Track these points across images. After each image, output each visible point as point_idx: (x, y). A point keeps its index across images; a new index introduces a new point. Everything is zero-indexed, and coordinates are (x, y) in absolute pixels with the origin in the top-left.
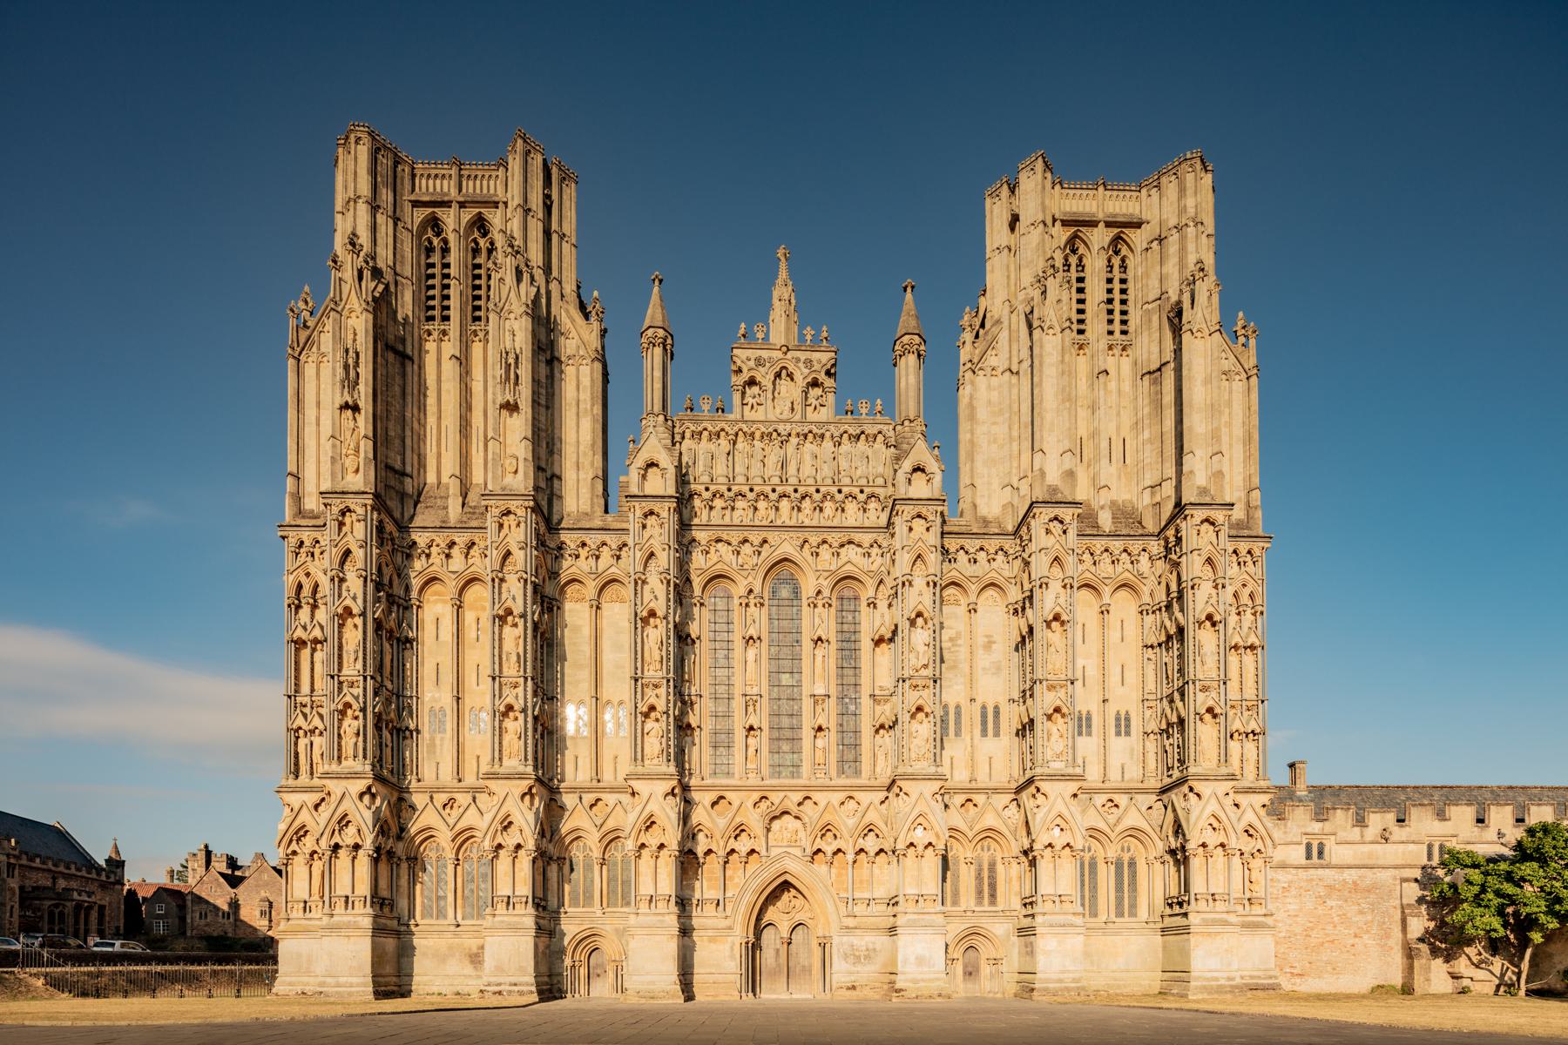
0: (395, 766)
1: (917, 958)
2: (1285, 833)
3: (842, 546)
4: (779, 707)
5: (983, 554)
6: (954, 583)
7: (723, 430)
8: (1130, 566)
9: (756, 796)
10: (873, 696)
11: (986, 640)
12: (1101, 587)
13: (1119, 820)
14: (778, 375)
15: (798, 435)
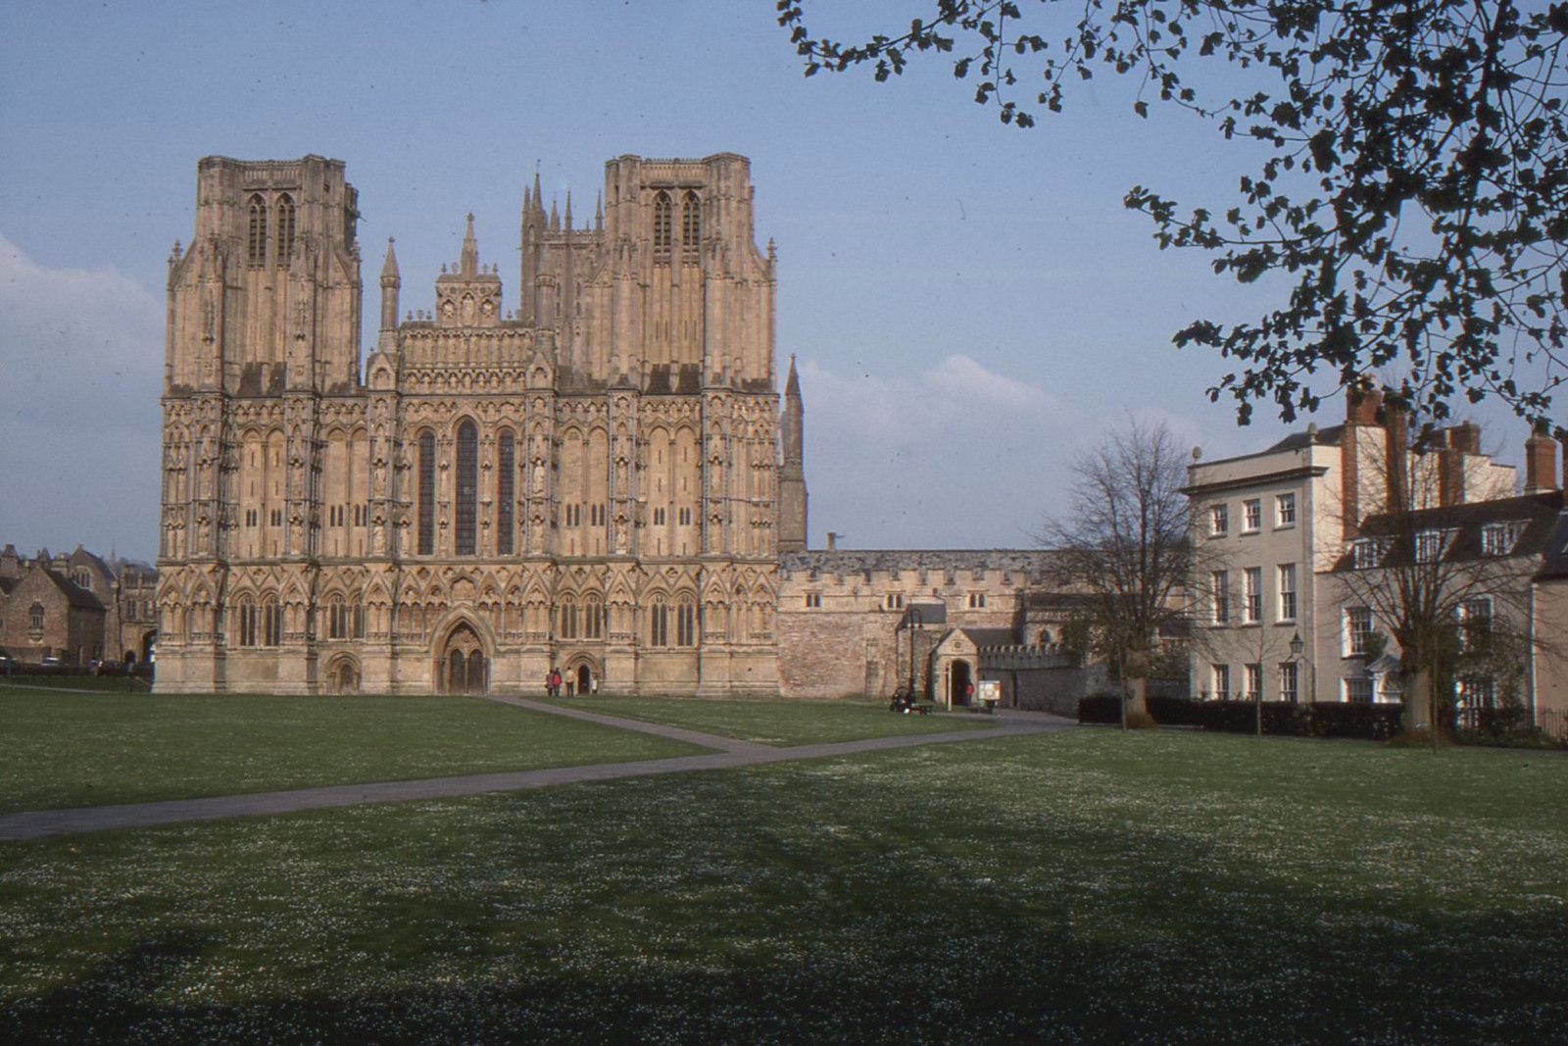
9: (444, 568)
13: (675, 583)
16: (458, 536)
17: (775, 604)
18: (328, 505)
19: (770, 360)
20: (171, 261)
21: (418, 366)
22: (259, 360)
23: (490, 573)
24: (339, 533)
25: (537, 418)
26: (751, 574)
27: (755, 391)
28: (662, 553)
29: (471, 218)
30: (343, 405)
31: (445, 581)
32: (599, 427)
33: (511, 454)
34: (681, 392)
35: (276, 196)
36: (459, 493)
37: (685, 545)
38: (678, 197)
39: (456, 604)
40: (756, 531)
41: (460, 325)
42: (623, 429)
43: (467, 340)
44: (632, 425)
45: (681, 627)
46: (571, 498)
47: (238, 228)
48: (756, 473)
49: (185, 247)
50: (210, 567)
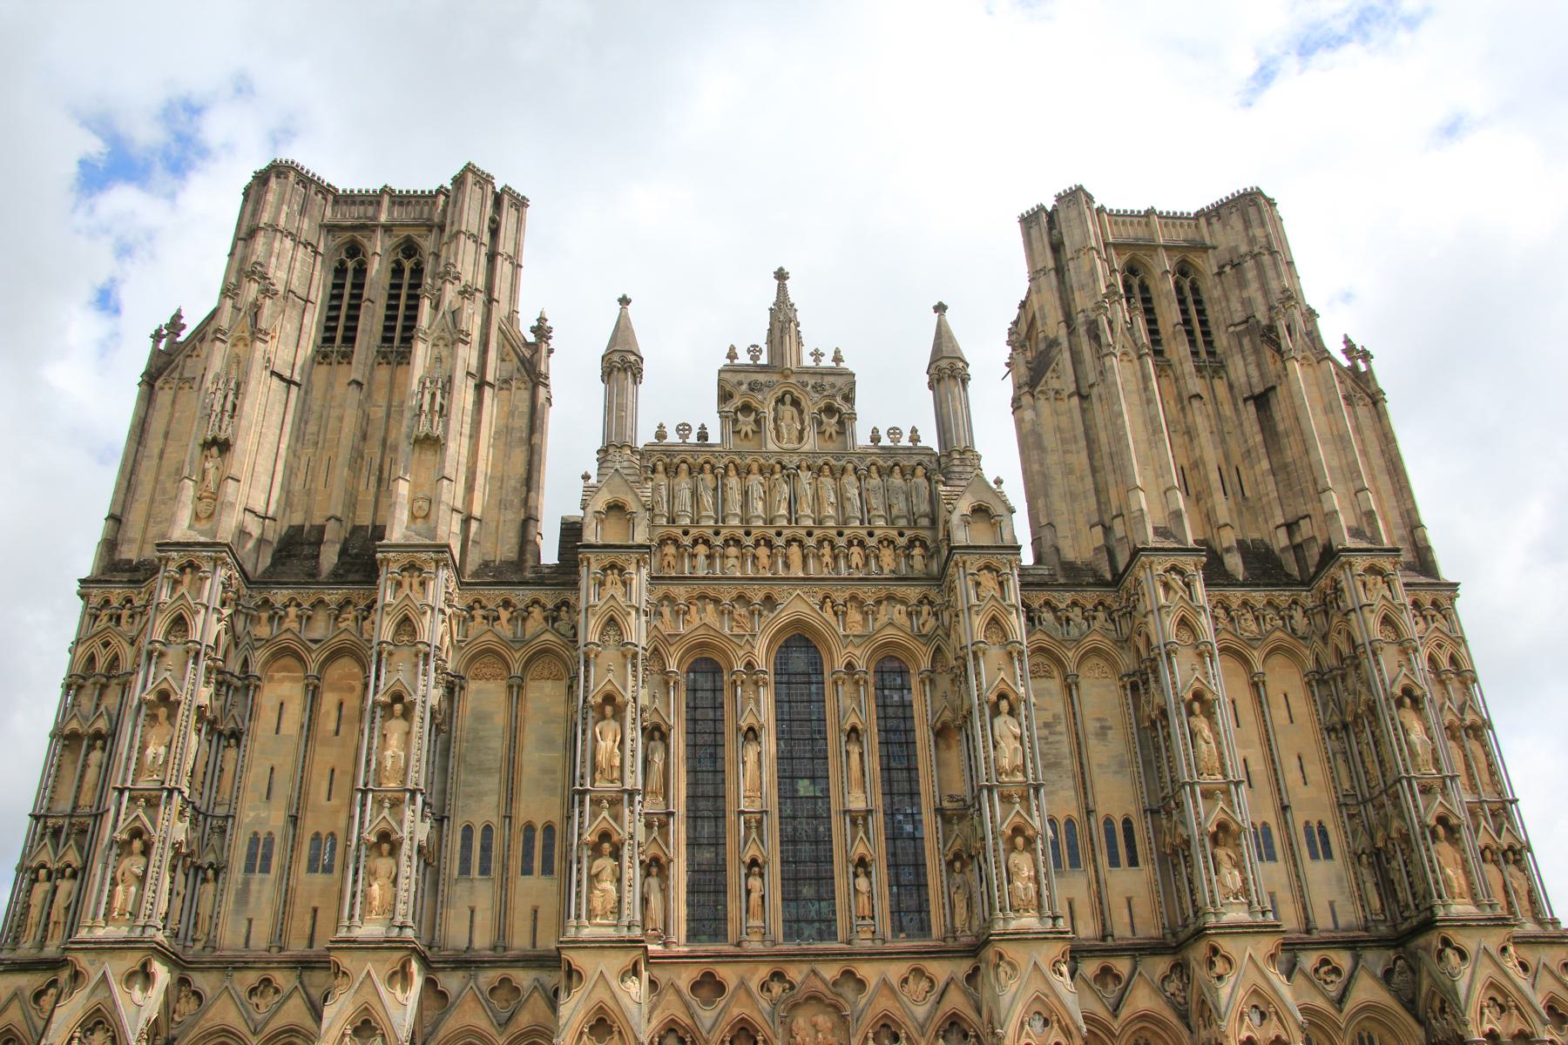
0: (183, 927)
3: (879, 602)
4: (795, 829)
5: (1077, 610)
7: (707, 462)
8: (1280, 622)
9: (764, 971)
10: (940, 811)
11: (1098, 725)
12: (1246, 652)
14: (780, 400)
20: (157, 336)
22: (318, 521)
23: (885, 982)
24: (483, 895)
25: (989, 608)
29: (781, 276)
30: (507, 604)
31: (765, 1005)
32: (1095, 651)
33: (906, 706)
36: (787, 793)
37: (1331, 904)
41: (771, 446)
42: (1185, 635)
43: (791, 478)
49: (192, 322)
50: (132, 961)
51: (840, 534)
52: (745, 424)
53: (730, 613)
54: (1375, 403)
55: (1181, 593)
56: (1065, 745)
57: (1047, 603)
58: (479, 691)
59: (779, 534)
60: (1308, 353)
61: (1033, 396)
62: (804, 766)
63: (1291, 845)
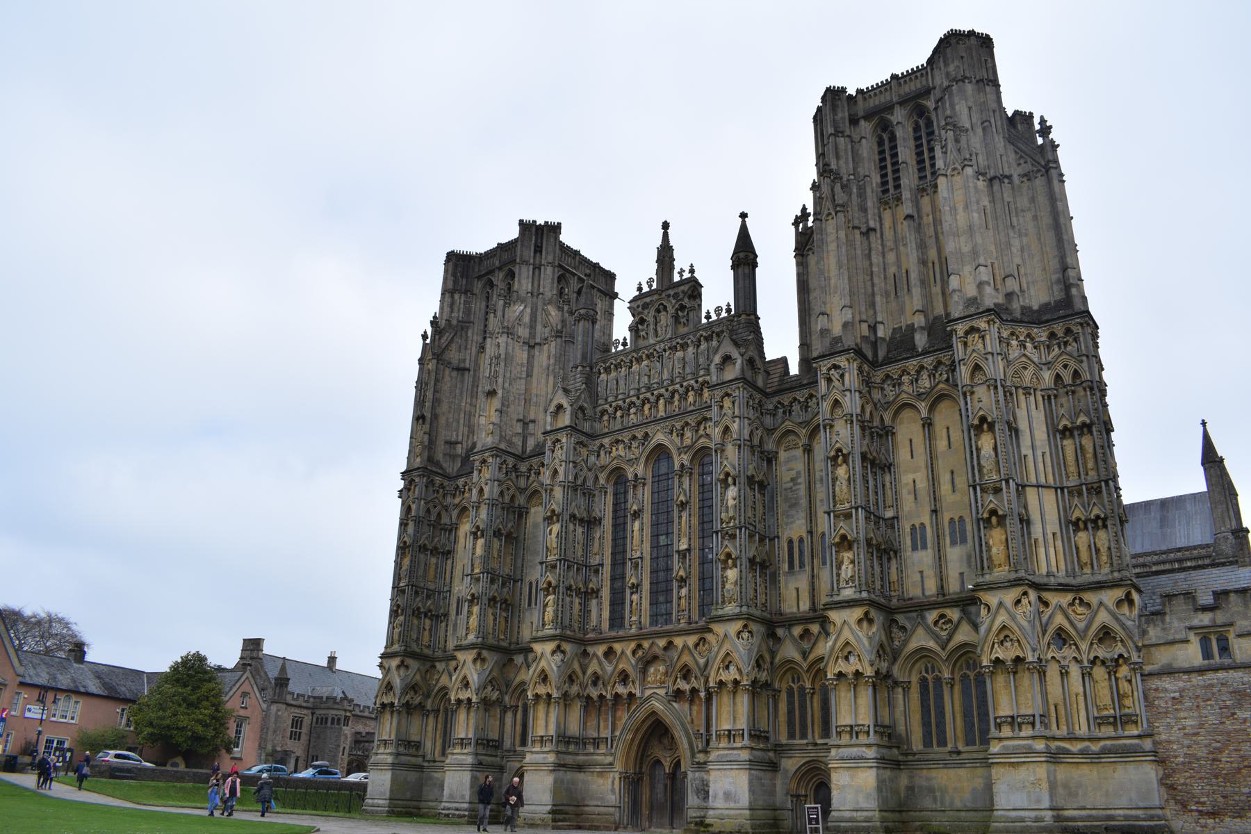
1: (725, 793)
2: (1164, 629)
3: (699, 424)
4: (658, 565)
6: (789, 432)
9: (633, 645)
12: (918, 404)
14: (658, 311)
15: (670, 348)
16: (654, 603)
17: (1135, 658)
18: (526, 581)
19: (1065, 268)
21: (610, 399)
23: (685, 646)
26: (1080, 610)
27: (1045, 318)
28: (927, 593)
29: (666, 226)
34: (926, 353)
35: (501, 275)
36: (655, 546)
37: (961, 574)
38: (899, 116)
39: (648, 693)
40: (1083, 538)
41: (652, 341)
44: (852, 403)
45: (967, 714)
46: (796, 528)
47: (468, 311)
48: (1068, 443)
51: (682, 386)
52: (643, 330)
53: (630, 448)
54: (1047, 172)
55: (837, 382)
56: (802, 490)
57: (795, 399)
58: (535, 513)
59: (652, 394)
60: (957, 165)
61: (802, 255)
62: (663, 528)
63: (938, 538)
